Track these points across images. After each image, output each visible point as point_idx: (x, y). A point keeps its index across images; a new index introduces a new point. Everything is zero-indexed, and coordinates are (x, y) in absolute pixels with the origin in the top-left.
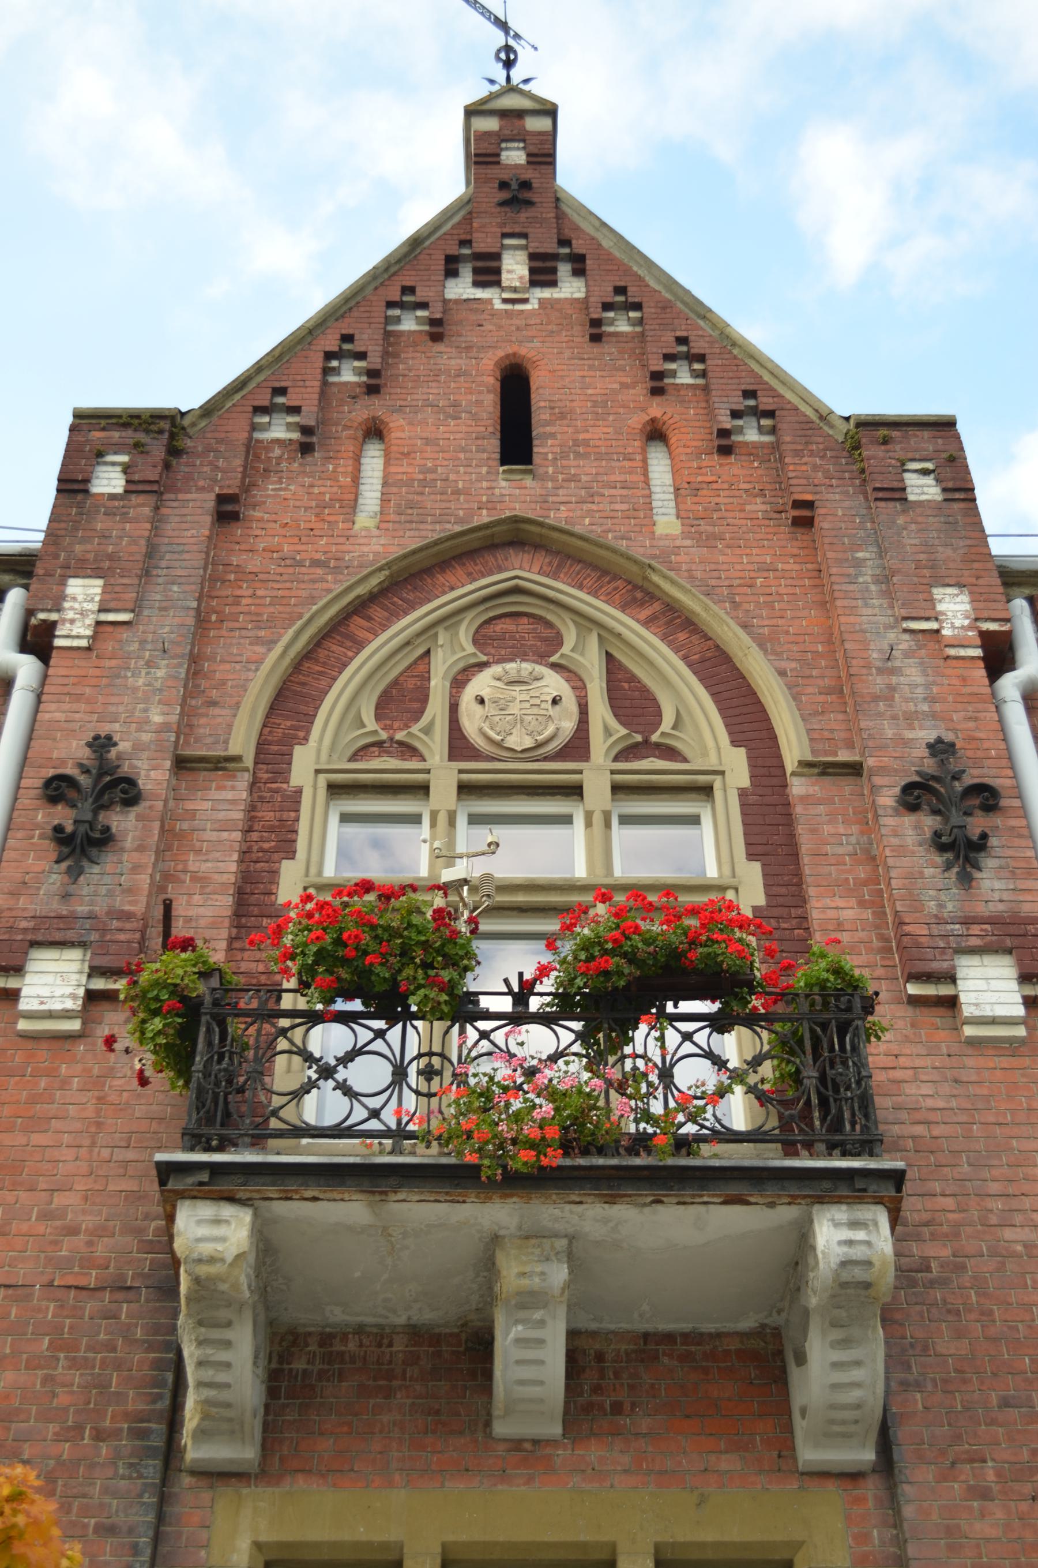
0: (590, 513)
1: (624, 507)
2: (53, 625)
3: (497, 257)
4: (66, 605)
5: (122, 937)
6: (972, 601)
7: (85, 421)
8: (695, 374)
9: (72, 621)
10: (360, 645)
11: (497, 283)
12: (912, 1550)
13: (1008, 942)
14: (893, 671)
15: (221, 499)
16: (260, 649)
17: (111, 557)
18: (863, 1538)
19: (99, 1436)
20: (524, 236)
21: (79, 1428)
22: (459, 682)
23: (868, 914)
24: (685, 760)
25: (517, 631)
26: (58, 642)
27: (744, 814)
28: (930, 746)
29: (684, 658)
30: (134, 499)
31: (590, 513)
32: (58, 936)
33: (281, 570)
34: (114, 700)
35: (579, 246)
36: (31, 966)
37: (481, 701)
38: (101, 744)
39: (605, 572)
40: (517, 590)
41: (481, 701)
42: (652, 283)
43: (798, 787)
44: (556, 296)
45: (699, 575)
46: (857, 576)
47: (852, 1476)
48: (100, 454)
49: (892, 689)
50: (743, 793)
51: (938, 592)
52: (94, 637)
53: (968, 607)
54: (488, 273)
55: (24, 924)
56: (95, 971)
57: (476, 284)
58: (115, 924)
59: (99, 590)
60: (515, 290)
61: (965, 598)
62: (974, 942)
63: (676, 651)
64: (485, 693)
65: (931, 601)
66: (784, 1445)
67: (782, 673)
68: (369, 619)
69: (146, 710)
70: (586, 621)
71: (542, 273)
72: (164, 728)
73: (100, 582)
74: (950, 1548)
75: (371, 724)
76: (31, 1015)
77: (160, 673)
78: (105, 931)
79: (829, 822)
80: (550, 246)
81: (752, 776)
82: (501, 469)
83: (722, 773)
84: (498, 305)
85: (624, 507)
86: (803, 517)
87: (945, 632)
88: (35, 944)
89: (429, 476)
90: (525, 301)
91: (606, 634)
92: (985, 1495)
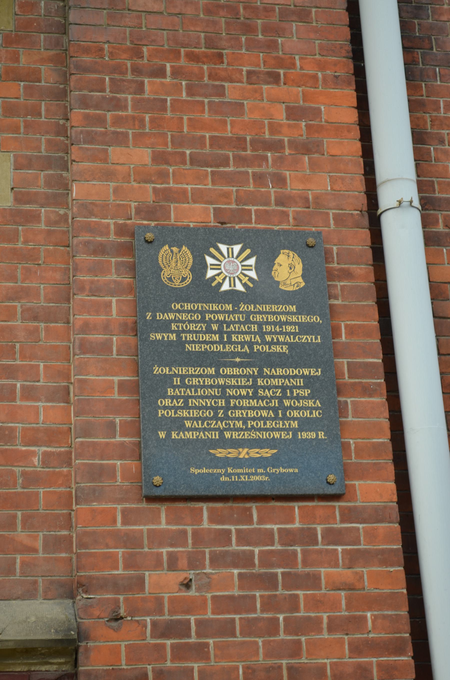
12: (73, 16)
74: (110, 16)
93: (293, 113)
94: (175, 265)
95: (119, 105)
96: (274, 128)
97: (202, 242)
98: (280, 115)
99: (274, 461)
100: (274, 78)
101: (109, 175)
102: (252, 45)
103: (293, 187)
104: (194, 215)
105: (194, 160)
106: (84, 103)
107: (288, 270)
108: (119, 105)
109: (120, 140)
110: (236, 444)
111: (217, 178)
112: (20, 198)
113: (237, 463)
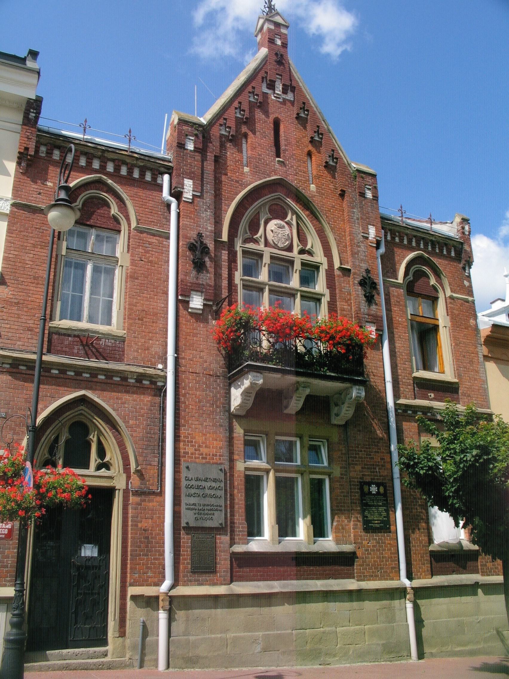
0: (296, 179)
1: (304, 179)
2: (182, 192)
3: (275, 82)
4: (185, 187)
5: (210, 291)
6: (376, 231)
7: (182, 122)
8: (319, 137)
9: (187, 193)
10: (246, 209)
11: (274, 90)
13: (375, 321)
14: (359, 247)
15: (215, 156)
16: (227, 207)
17: (193, 173)
18: (340, 436)
19: (217, 407)
20: (281, 75)
21: (213, 404)
22: (266, 223)
23: (349, 308)
24: (313, 256)
25: (279, 212)
26: (184, 199)
27: (326, 276)
28: (366, 270)
29: (315, 229)
30: (197, 154)
31: (296, 179)
32: (196, 289)
33: (228, 182)
34: (198, 220)
35: (294, 84)
36: (192, 296)
37: (272, 231)
38: (200, 235)
39: (298, 198)
40: (279, 198)
41: (272, 231)
42: (312, 103)
43: (337, 273)
44: (287, 98)
45: (319, 205)
46: (354, 216)
47: (339, 426)
48: (187, 135)
49: (359, 251)
50: (326, 270)
51: (370, 227)
52: (193, 199)
53: (374, 232)
54: (271, 86)
55: (189, 284)
56: (205, 299)
57: (268, 88)
58: (208, 288)
59: (192, 183)
60: (278, 94)
61: (374, 229)
62: (369, 320)
63: (314, 226)
64: (273, 229)
65: (368, 228)
66: (329, 419)
67: (336, 240)
68: (248, 201)
69: (206, 225)
70: (294, 212)
71: (285, 91)
72: (211, 231)
73: (192, 181)
75: (249, 234)
76: (192, 308)
77: (208, 214)
78: (206, 289)
79: (343, 283)
80: (288, 83)
81: (328, 266)
82: (277, 159)
83: (322, 264)
84: (273, 98)
85: (304, 179)
86: (342, 194)
87: (370, 238)
88: (192, 290)
89: (260, 157)
90: (279, 98)
91: (298, 217)
92: (359, 431)
93: (382, 459)
94: (366, 488)
95: (356, 458)
96: (379, 462)
97: (369, 484)
98: (379, 460)
99: (380, 523)
100: (378, 452)
101: (356, 471)
102: (375, 445)
103: (382, 474)
104: (368, 479)
105: (368, 468)
106: (351, 457)
107: (382, 490)
108: (356, 458)
109: (356, 464)
110: (375, 520)
111: (371, 472)
112: (341, 474)
113: (375, 524)
